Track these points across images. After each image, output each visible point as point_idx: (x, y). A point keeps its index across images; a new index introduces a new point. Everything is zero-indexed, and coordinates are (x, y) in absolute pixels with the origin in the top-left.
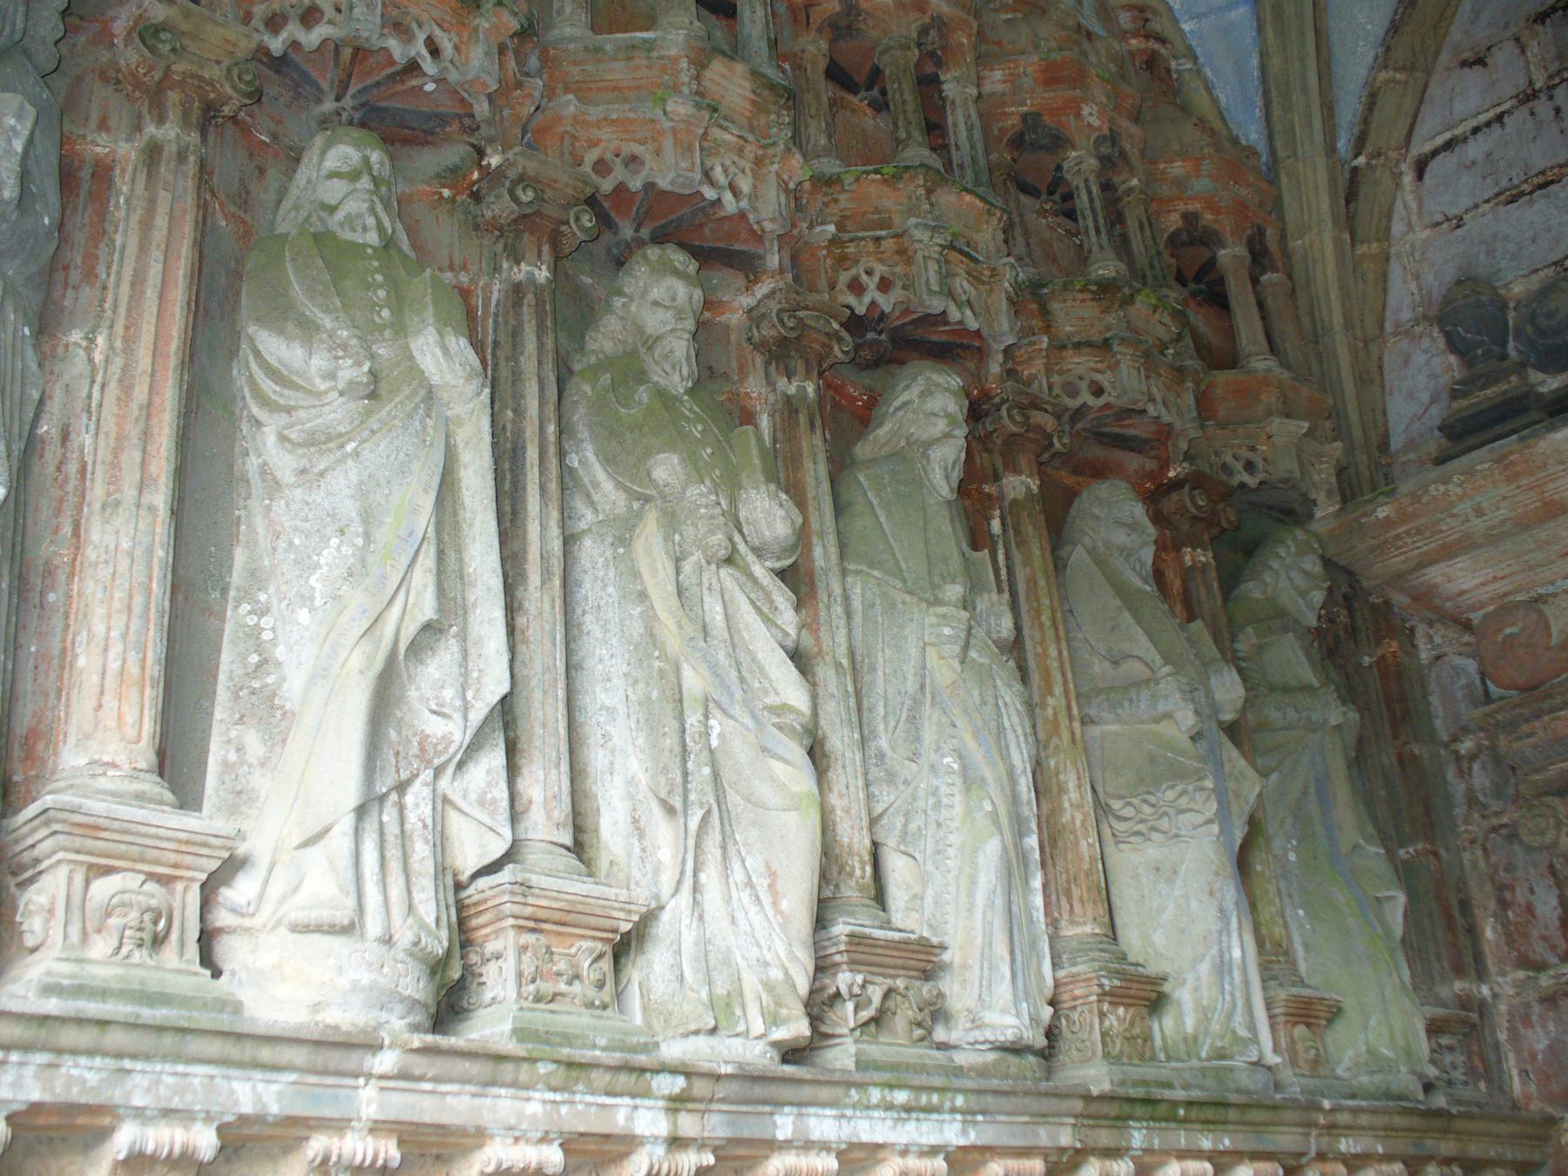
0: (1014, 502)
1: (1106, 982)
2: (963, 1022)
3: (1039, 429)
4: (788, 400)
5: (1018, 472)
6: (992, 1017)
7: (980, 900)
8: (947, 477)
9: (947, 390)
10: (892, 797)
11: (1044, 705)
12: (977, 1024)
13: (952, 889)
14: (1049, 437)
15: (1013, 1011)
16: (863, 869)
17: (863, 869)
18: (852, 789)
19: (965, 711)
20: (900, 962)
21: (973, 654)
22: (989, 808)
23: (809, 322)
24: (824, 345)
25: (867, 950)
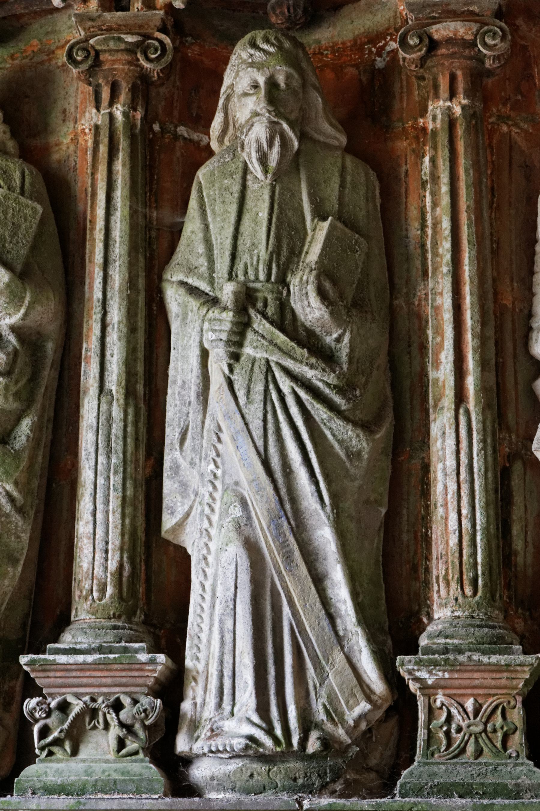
0: (434, 133)
1: (423, 674)
2: (204, 732)
3: (449, 41)
4: (97, 127)
5: (437, 96)
6: (229, 725)
7: (218, 609)
8: (263, 160)
9: (252, 65)
10: (186, 508)
11: (437, 365)
12: (214, 733)
13: (208, 596)
14: (473, 44)
15: (256, 719)
16: (103, 590)
17: (103, 590)
18: (100, 516)
19: (227, 416)
20: (109, 681)
21: (248, 351)
22: (237, 512)
23: (98, 48)
24: (130, 63)
25: (58, 674)
